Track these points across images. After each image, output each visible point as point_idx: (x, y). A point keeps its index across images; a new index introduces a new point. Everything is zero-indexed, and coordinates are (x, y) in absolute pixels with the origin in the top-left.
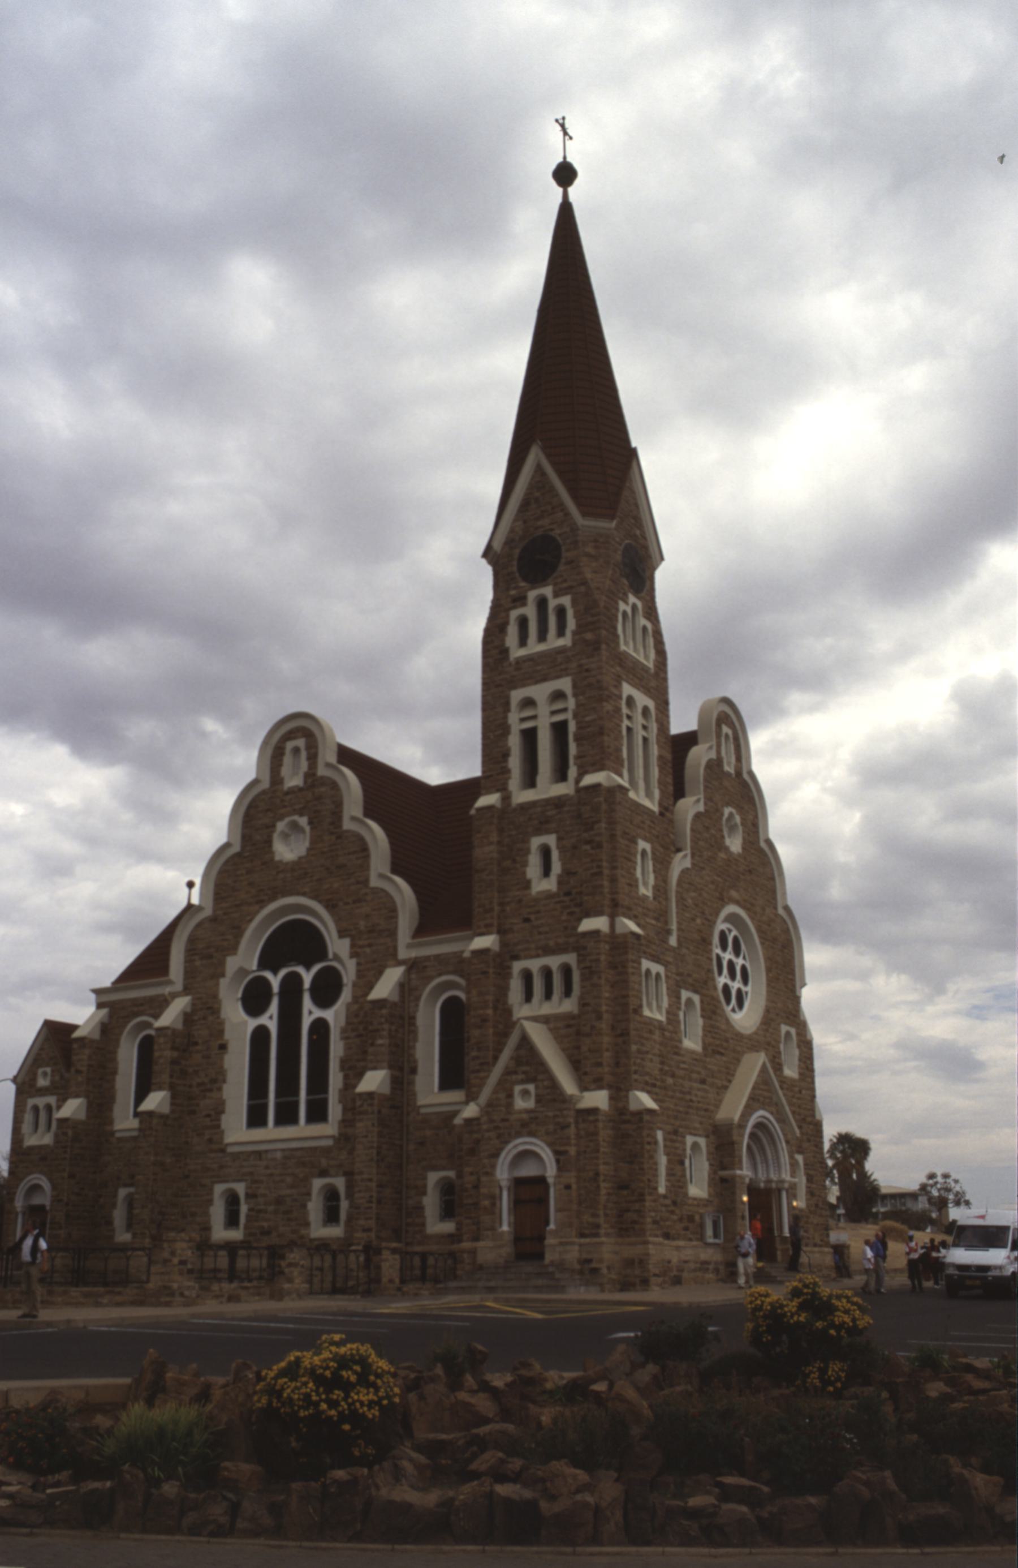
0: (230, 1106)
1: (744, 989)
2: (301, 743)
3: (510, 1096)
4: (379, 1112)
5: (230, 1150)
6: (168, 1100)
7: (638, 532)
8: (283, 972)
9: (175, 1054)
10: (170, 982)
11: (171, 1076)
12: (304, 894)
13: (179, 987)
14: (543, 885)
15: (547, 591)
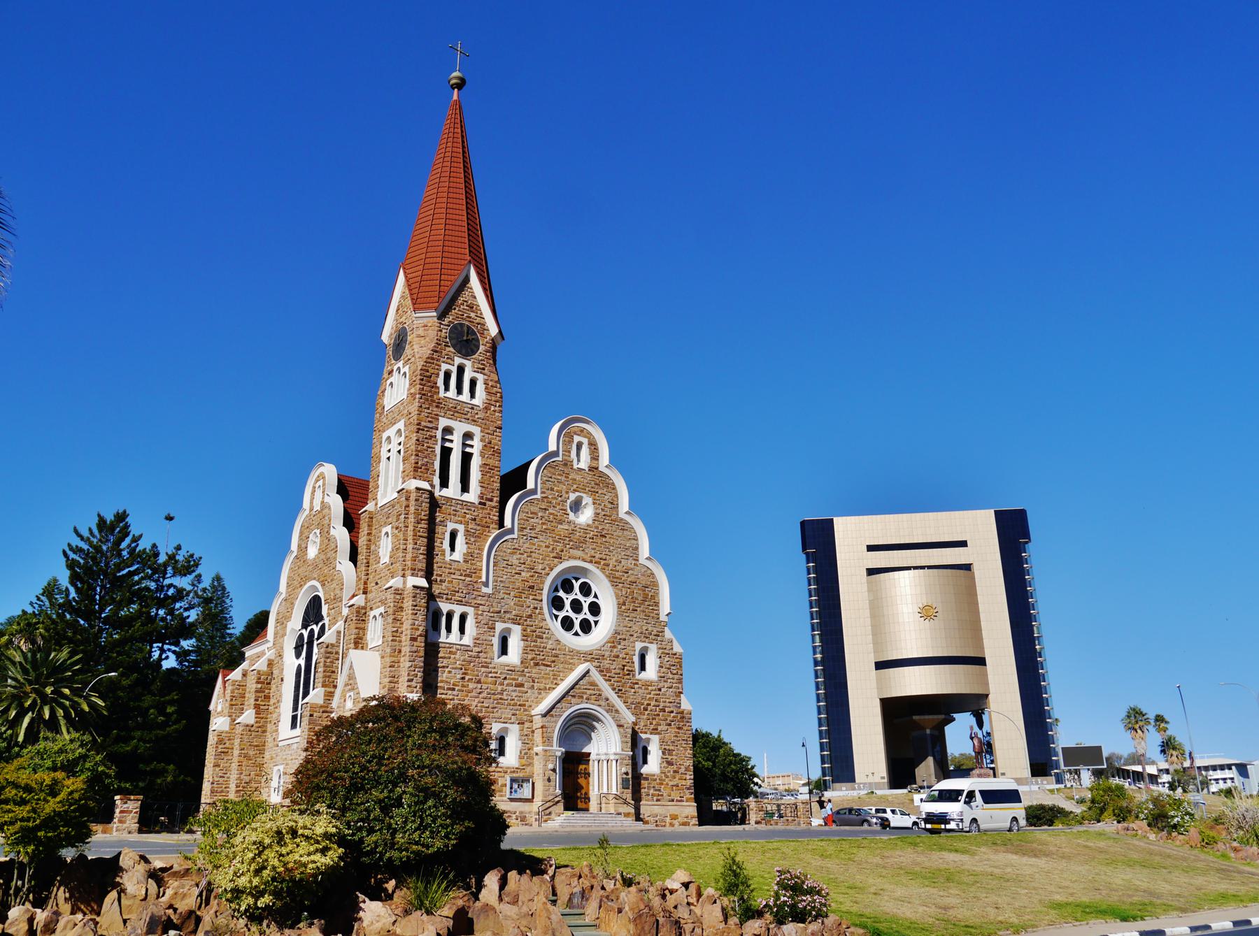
0: (282, 718)
1: (591, 619)
2: (320, 483)
3: (345, 701)
4: (311, 715)
5: (281, 744)
6: (254, 716)
7: (473, 315)
8: (309, 628)
9: (259, 686)
10: (267, 641)
11: (256, 700)
12: (315, 579)
13: (270, 645)
14: (385, 558)
15: (400, 364)
